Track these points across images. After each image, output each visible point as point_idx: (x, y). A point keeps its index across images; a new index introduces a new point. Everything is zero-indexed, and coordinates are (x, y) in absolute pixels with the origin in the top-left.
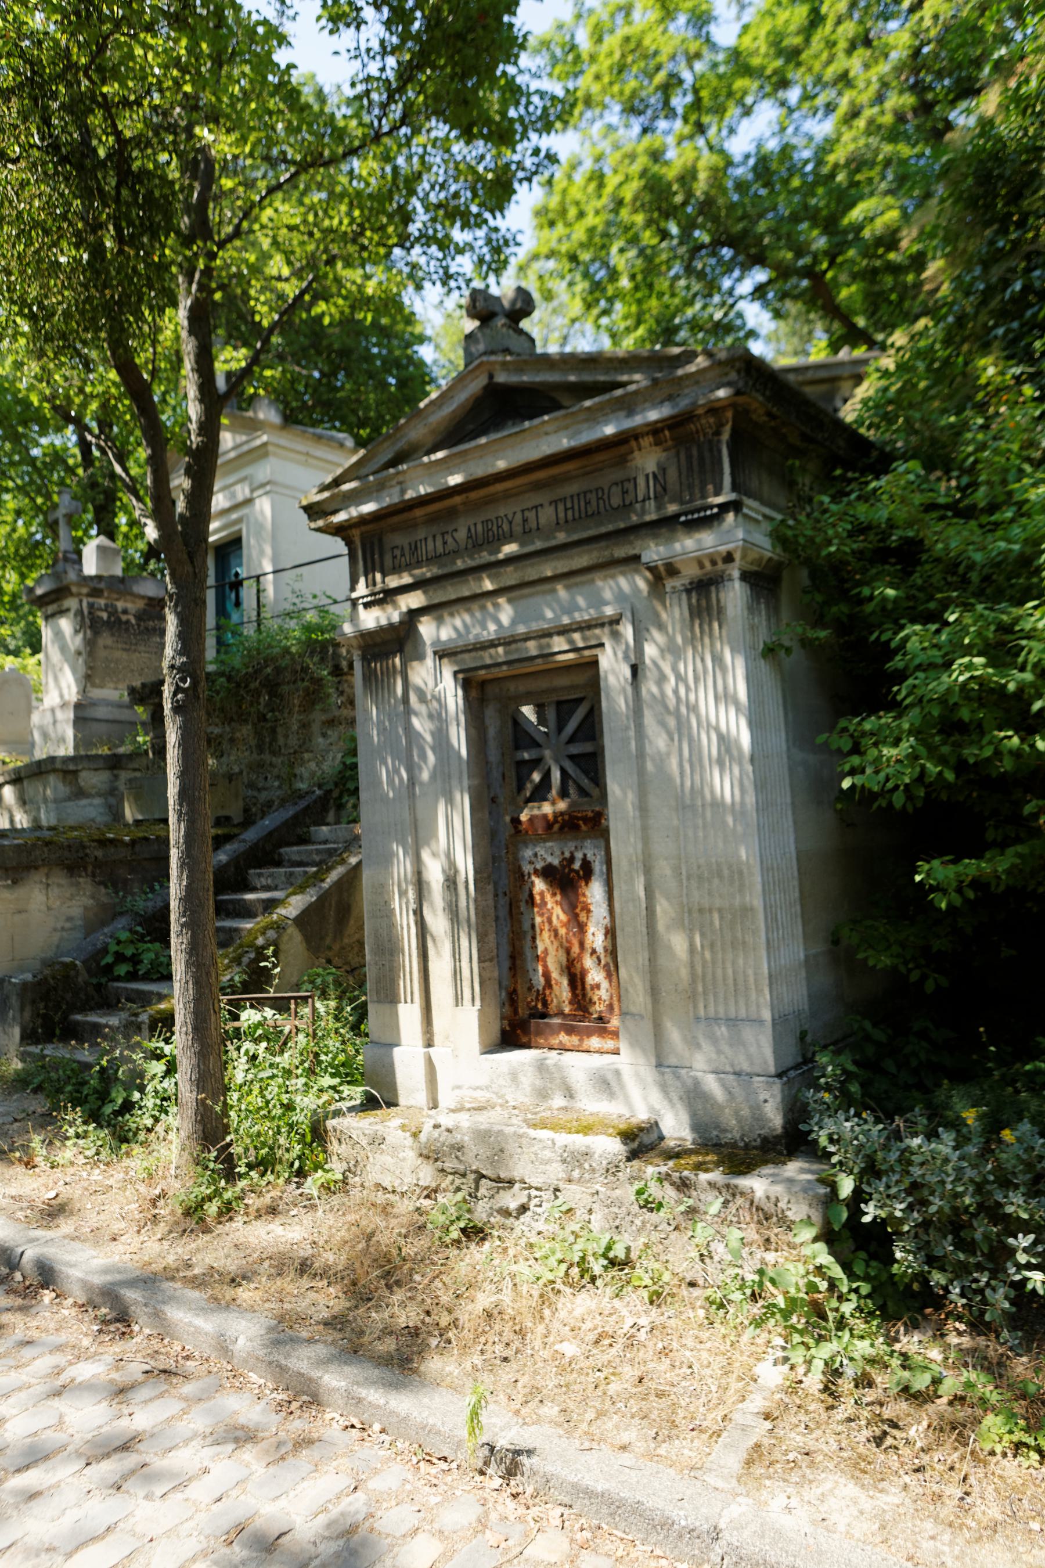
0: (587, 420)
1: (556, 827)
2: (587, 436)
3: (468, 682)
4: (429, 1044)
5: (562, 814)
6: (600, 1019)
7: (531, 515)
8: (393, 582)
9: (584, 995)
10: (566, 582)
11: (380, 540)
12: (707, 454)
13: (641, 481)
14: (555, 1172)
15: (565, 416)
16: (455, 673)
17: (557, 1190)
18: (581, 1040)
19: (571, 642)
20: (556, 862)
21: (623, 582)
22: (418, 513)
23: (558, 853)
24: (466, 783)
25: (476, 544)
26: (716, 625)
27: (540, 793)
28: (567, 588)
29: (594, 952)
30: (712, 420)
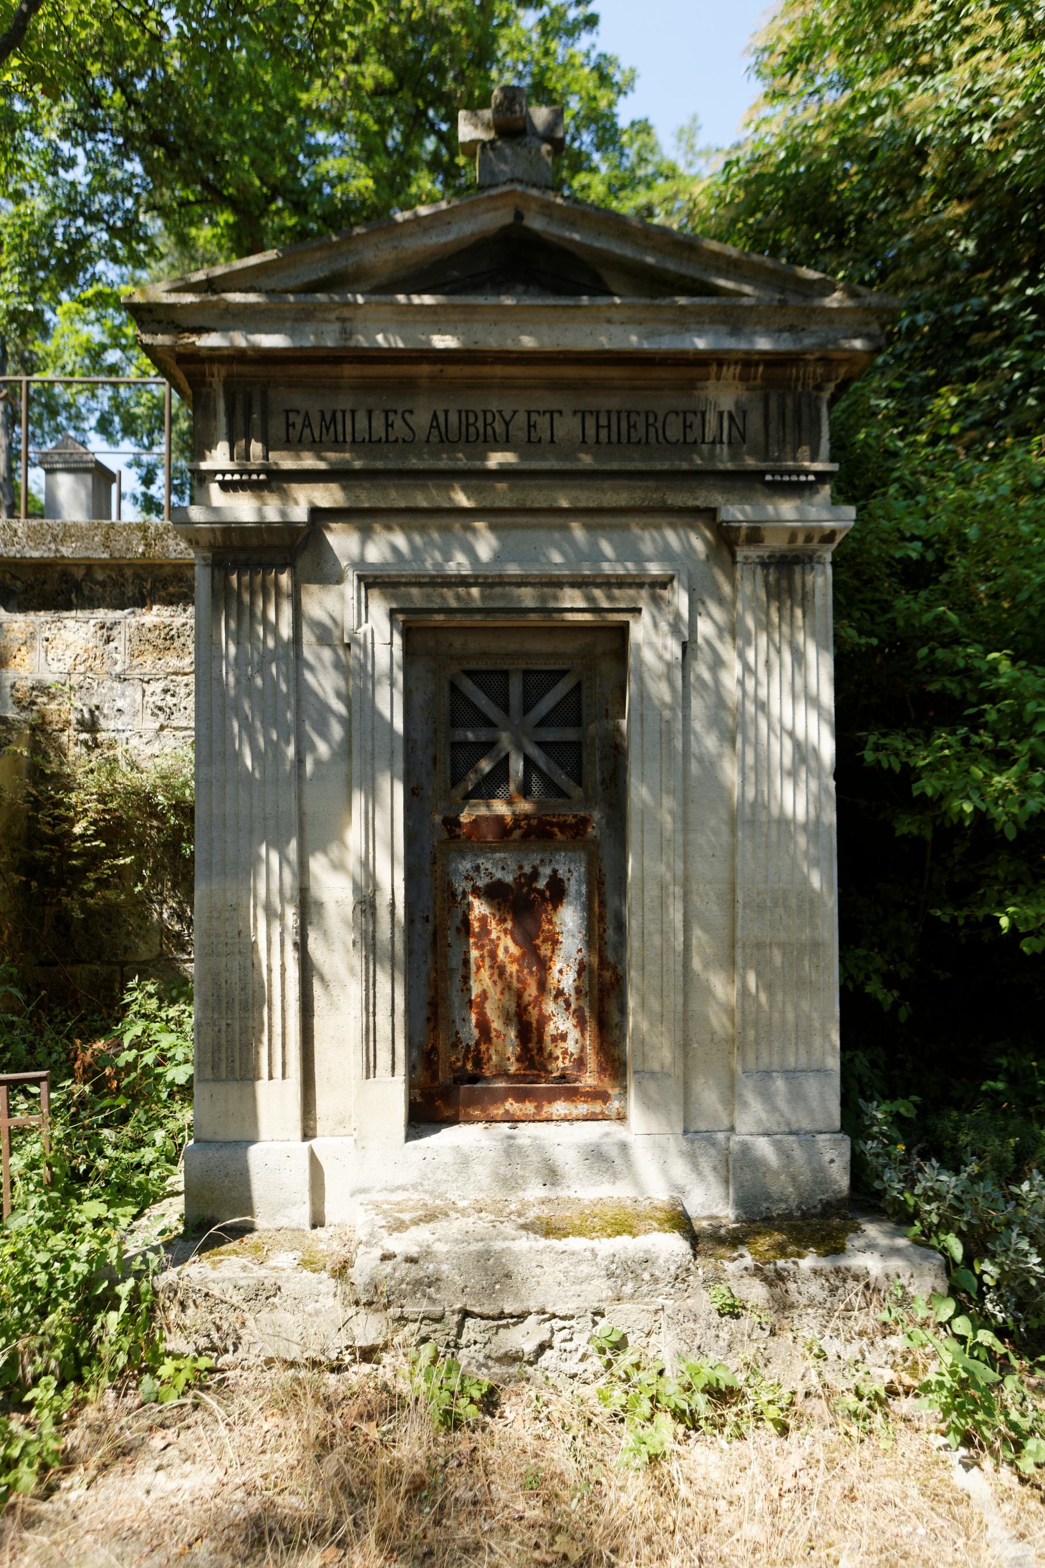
0: (673, 322)
1: (517, 834)
2: (668, 342)
3: (411, 627)
4: (308, 1134)
5: (527, 817)
6: (563, 1077)
7: (543, 422)
8: (287, 462)
9: (541, 1049)
10: (587, 520)
11: (264, 394)
12: (805, 409)
13: (712, 419)
14: (599, 1290)
15: (647, 307)
16: (392, 613)
17: (599, 1313)
18: (539, 1108)
19: (590, 598)
20: (509, 879)
21: (671, 537)
22: (349, 371)
23: (513, 866)
24: (400, 766)
25: (443, 438)
26: (799, 613)
27: (491, 785)
28: (587, 527)
29: (560, 993)
30: (820, 371)
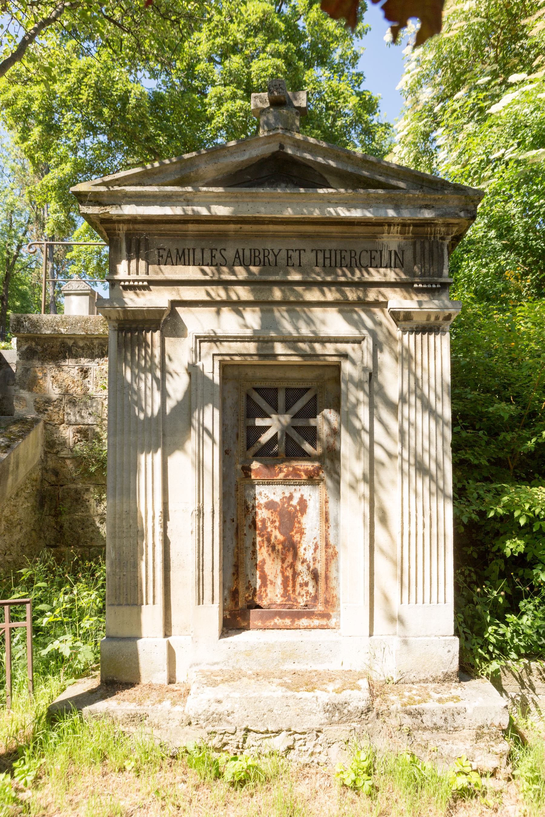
4: (167, 633)
7: (295, 255)
12: (435, 249)
13: (386, 255)
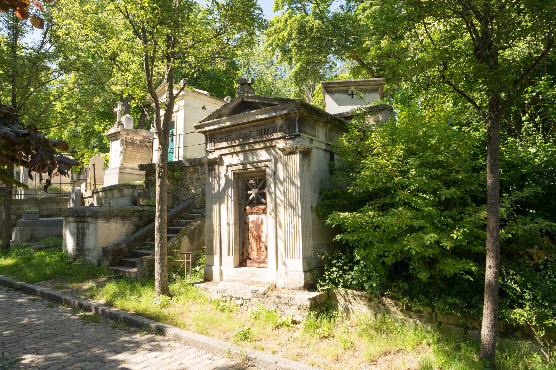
4: (221, 266)
7: (251, 133)
13: (278, 128)
